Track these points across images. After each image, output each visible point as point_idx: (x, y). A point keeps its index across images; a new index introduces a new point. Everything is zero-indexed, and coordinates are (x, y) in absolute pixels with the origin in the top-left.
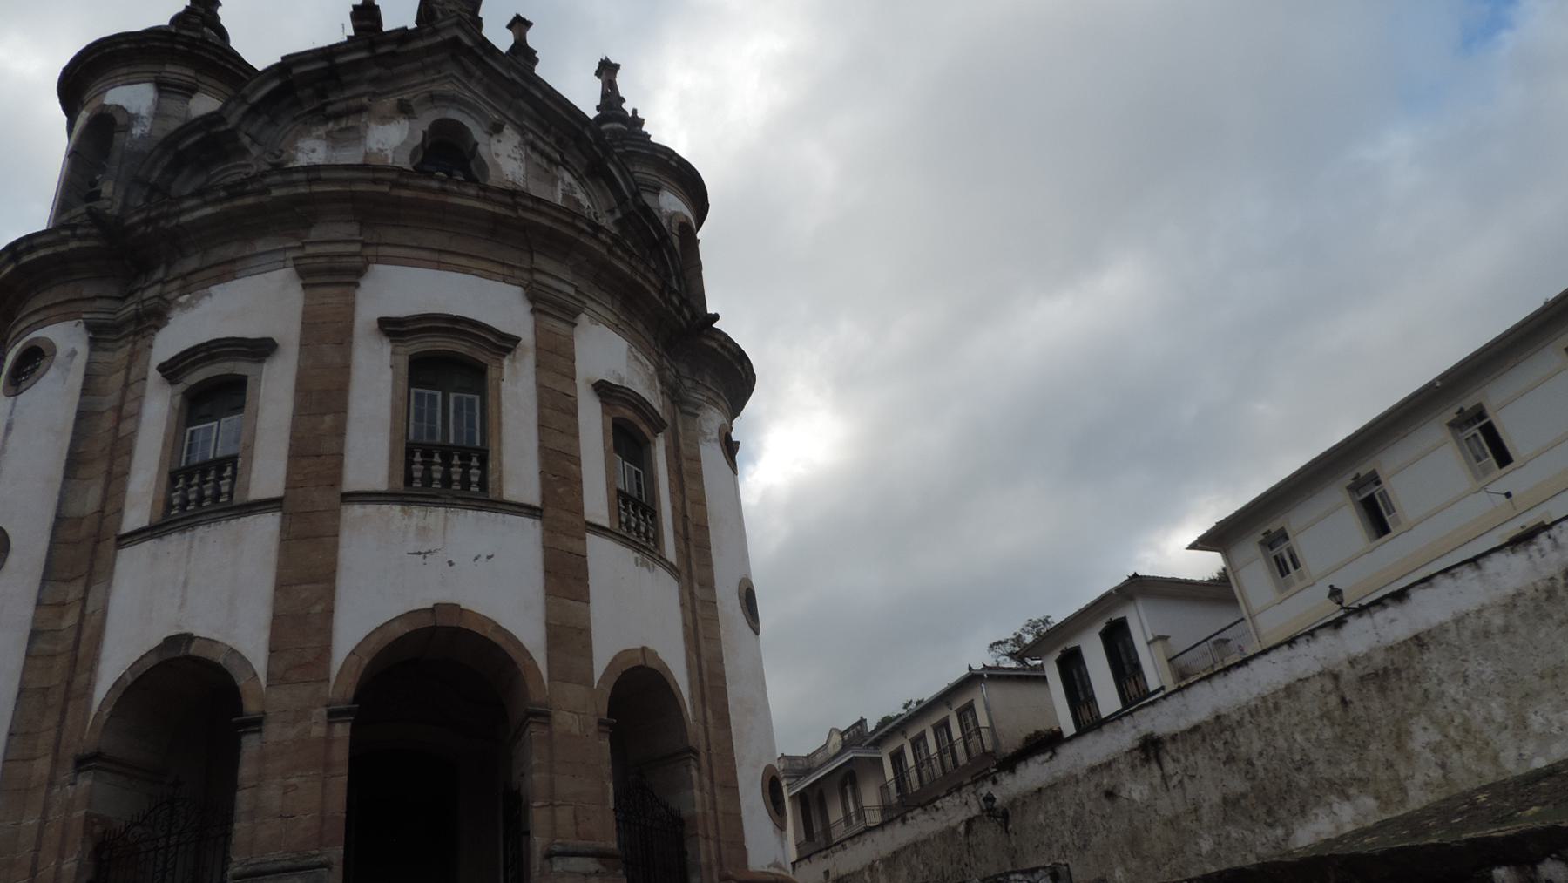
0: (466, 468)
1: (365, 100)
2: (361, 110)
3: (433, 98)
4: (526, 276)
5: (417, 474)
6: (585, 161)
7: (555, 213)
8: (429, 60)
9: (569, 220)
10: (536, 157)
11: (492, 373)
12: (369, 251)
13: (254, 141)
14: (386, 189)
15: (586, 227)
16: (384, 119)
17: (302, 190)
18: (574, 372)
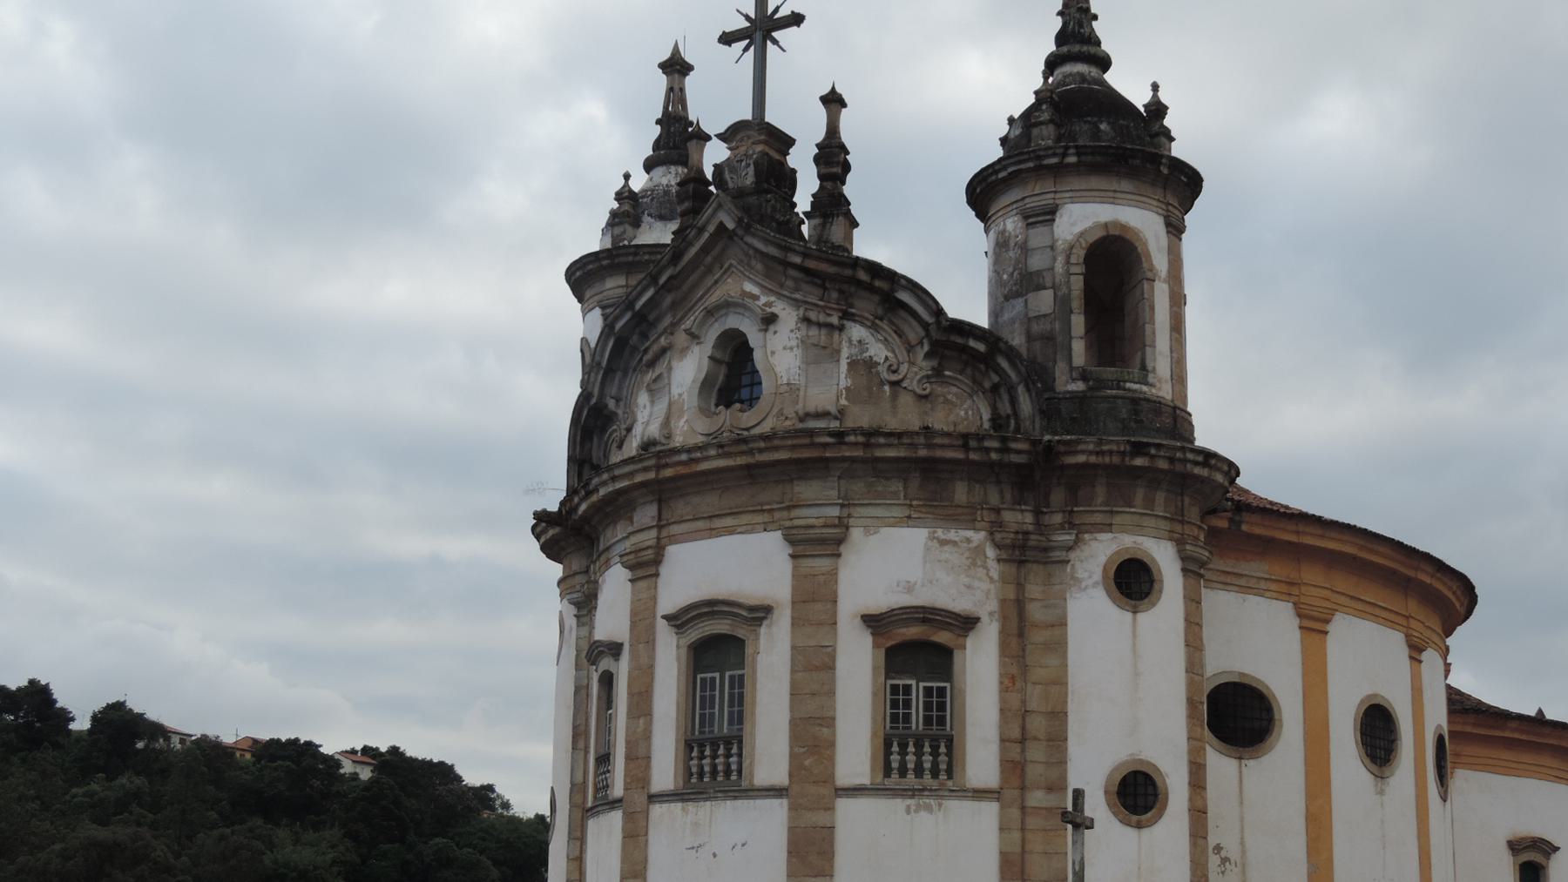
0: (728, 755)
1: (663, 341)
2: (664, 351)
3: (711, 313)
4: (785, 514)
5: (694, 770)
6: (876, 298)
7: (789, 442)
8: (709, 259)
9: (807, 441)
10: (814, 331)
11: (749, 650)
12: (664, 533)
13: (618, 400)
14: (652, 475)
15: (829, 440)
16: (684, 351)
17: (610, 488)
18: (835, 614)
